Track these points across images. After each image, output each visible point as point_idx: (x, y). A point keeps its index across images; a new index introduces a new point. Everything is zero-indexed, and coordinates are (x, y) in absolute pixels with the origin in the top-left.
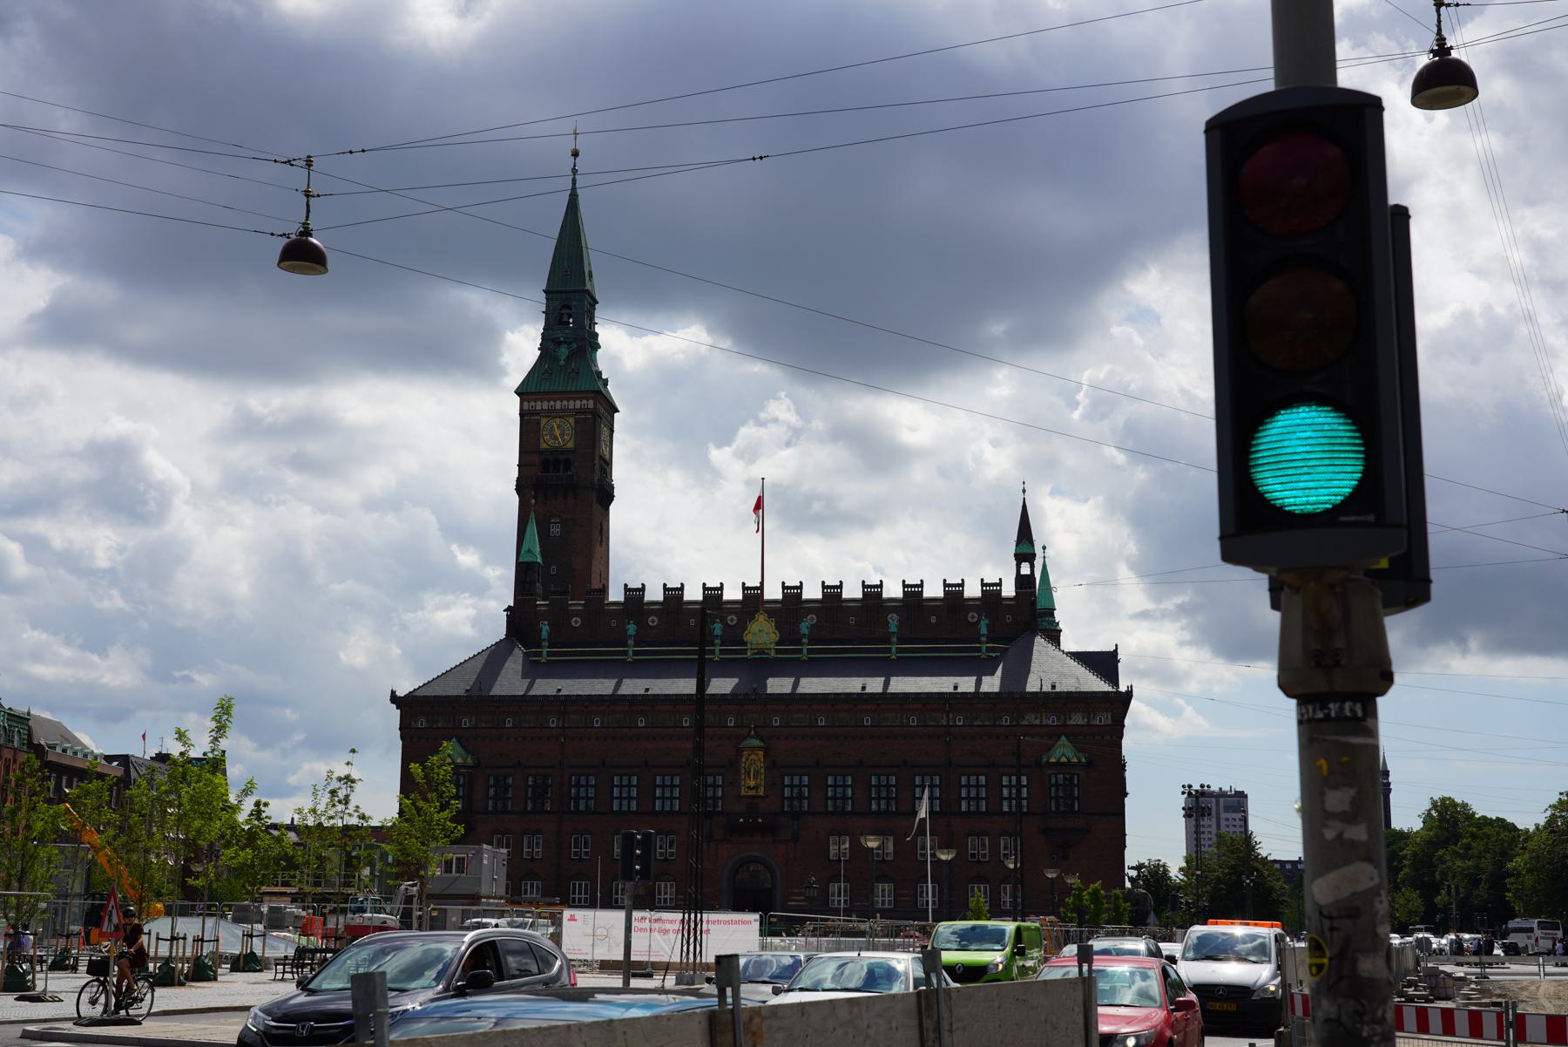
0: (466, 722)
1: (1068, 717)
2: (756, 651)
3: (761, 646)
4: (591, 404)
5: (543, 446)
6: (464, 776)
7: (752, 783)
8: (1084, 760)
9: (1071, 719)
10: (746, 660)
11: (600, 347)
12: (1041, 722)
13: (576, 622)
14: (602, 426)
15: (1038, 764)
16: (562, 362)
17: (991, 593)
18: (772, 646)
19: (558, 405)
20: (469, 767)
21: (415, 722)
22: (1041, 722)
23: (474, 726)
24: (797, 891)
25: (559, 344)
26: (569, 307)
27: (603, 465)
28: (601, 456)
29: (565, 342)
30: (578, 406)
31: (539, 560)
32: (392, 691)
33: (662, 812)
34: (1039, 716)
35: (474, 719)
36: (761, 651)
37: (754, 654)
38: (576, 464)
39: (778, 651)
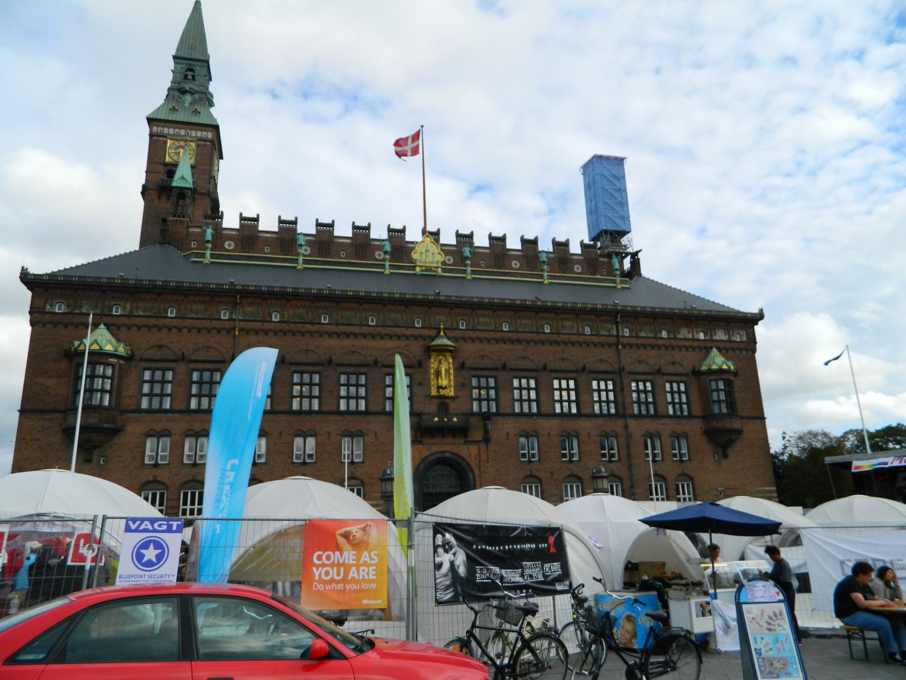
0: (117, 311)
1: (713, 333)
2: (424, 268)
3: (428, 265)
4: (210, 135)
5: (168, 159)
6: (113, 366)
7: (444, 382)
8: (732, 368)
9: (715, 334)
10: (415, 274)
11: (214, 106)
12: (693, 336)
13: (229, 245)
15: (697, 373)
16: (187, 105)
18: (440, 265)
19: (183, 132)
21: (51, 305)
22: (693, 336)
23: (128, 313)
25: (183, 92)
26: (192, 70)
33: (348, 412)
34: (690, 330)
35: (128, 305)
36: (429, 269)
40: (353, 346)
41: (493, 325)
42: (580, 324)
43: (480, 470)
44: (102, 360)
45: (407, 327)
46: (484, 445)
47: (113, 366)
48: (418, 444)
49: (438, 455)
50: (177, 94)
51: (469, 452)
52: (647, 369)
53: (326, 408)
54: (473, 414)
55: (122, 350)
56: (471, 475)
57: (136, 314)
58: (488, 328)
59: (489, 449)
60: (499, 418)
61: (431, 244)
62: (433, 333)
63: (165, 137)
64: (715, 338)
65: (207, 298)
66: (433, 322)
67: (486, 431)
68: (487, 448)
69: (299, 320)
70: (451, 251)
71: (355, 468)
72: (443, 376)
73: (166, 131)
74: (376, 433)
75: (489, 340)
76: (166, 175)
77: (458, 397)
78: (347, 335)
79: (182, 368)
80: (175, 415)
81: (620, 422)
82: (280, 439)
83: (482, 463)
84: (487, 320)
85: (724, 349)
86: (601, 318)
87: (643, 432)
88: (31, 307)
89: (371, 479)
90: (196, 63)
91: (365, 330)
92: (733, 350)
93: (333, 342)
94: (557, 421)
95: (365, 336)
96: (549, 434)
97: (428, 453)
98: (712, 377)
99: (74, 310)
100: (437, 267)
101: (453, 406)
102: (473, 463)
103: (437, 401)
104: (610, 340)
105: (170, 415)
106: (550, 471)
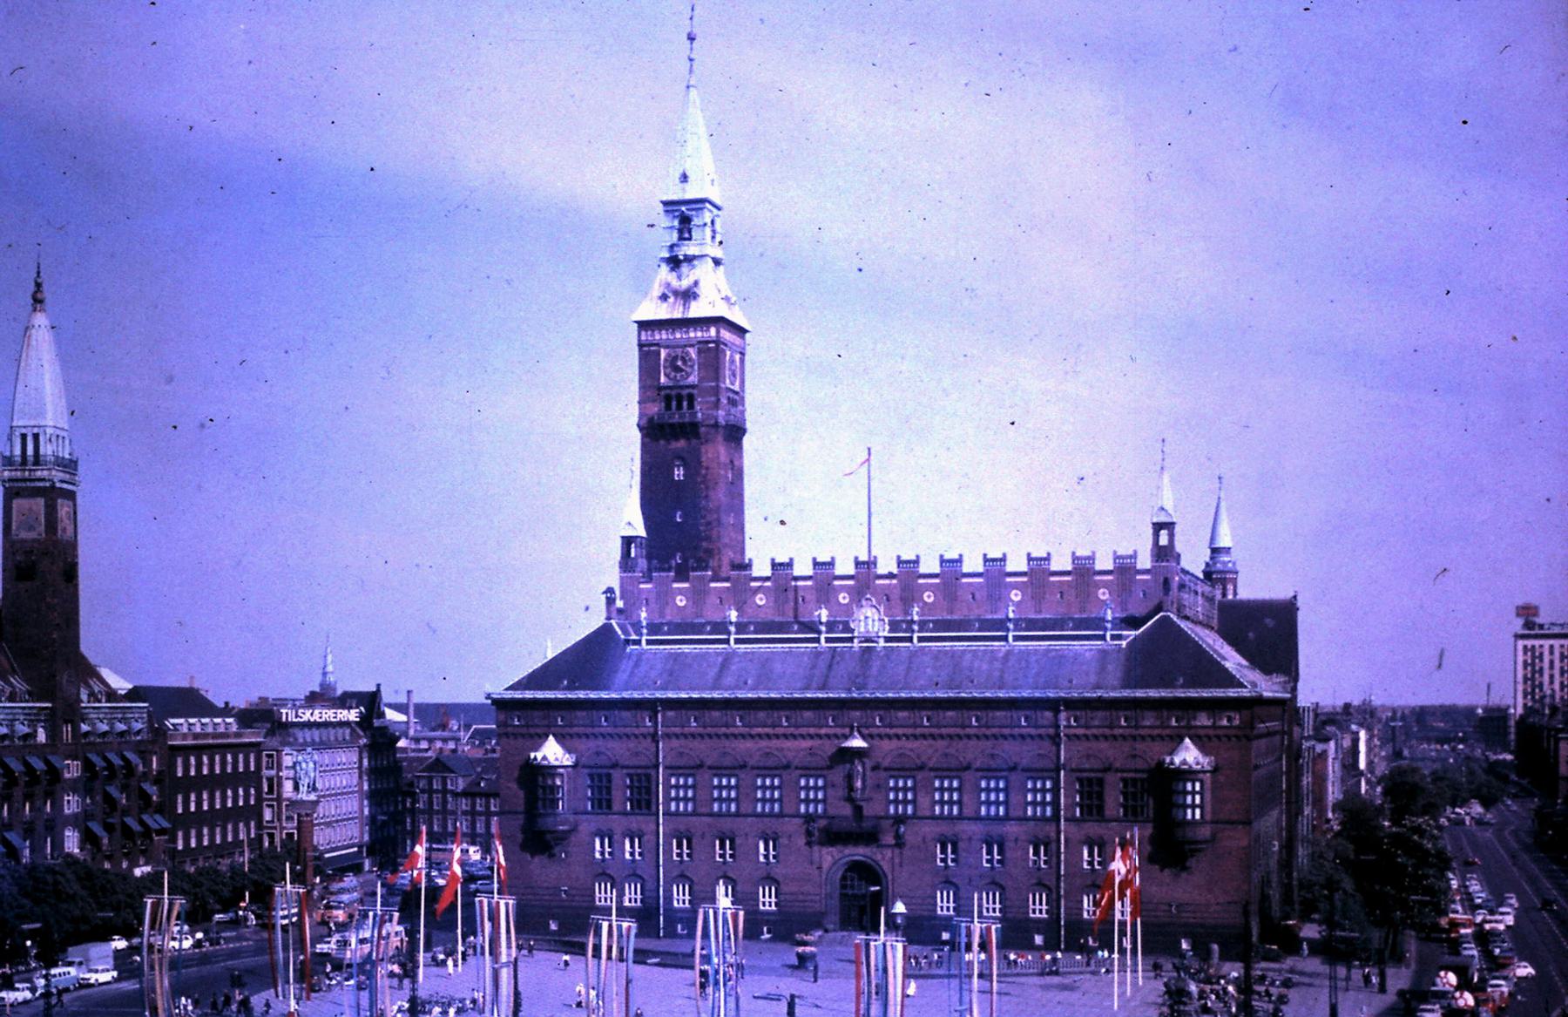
13: (681, 601)
14: (728, 353)
17: (1124, 569)
27: (731, 395)
31: (643, 533)
36: (868, 640)
37: (861, 642)
39: (888, 640)
47: (562, 775)
51: (883, 857)
53: (743, 811)
55: (568, 760)
62: (847, 731)
63: (657, 345)
64: (1193, 723)
70: (931, 585)
75: (907, 737)
92: (1218, 737)
93: (749, 744)
95: (777, 736)
97: (840, 855)
102: (886, 867)
104: (1051, 731)
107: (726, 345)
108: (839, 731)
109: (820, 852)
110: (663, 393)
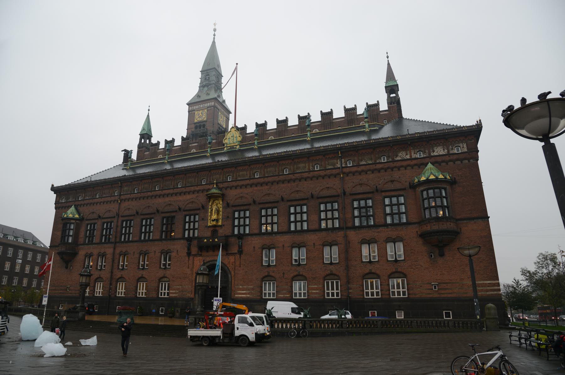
2: (229, 147)
3: (232, 145)
4: (213, 103)
5: (196, 121)
6: (73, 223)
7: (214, 217)
14: (220, 113)
19: (201, 106)
20: (76, 219)
21: (61, 200)
24: (241, 287)
28: (218, 123)
29: (206, 86)
30: (208, 105)
32: (52, 185)
36: (232, 147)
38: (207, 125)
40: (170, 201)
41: (249, 176)
42: (311, 164)
43: (234, 272)
44: (69, 222)
45: (197, 186)
46: (238, 256)
48: (199, 256)
49: (211, 263)
50: (201, 88)
52: (366, 189)
54: (233, 235)
55: (77, 216)
56: (230, 276)
57: (86, 198)
58: (245, 178)
59: (241, 258)
60: (249, 237)
61: (235, 132)
62: (211, 186)
65: (110, 186)
66: (211, 180)
67: (240, 247)
68: (240, 257)
69: (145, 191)
71: (166, 271)
72: (213, 213)
73: (195, 108)
74: (177, 251)
75: (246, 186)
76: (194, 129)
77: (224, 225)
78: (168, 195)
79: (99, 222)
80: (96, 245)
81: (341, 233)
82: (134, 256)
83: (236, 268)
84: (245, 173)
85: (438, 163)
86: (328, 157)
87: (360, 240)
88: (55, 202)
89: (173, 278)
90: (210, 71)
91: (176, 191)
93: (160, 201)
94: (290, 236)
95: (176, 194)
96: (283, 246)
98: (422, 188)
99: (67, 200)
100: (237, 145)
101: (221, 232)
103: (212, 229)
104: (334, 172)
105: (94, 245)
106: (283, 272)
107: (219, 110)
108: (208, 187)
109: (193, 260)
110: (196, 125)
